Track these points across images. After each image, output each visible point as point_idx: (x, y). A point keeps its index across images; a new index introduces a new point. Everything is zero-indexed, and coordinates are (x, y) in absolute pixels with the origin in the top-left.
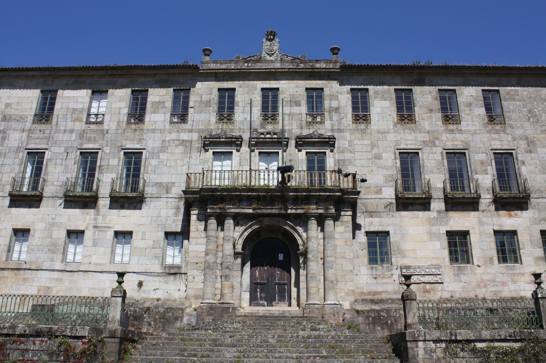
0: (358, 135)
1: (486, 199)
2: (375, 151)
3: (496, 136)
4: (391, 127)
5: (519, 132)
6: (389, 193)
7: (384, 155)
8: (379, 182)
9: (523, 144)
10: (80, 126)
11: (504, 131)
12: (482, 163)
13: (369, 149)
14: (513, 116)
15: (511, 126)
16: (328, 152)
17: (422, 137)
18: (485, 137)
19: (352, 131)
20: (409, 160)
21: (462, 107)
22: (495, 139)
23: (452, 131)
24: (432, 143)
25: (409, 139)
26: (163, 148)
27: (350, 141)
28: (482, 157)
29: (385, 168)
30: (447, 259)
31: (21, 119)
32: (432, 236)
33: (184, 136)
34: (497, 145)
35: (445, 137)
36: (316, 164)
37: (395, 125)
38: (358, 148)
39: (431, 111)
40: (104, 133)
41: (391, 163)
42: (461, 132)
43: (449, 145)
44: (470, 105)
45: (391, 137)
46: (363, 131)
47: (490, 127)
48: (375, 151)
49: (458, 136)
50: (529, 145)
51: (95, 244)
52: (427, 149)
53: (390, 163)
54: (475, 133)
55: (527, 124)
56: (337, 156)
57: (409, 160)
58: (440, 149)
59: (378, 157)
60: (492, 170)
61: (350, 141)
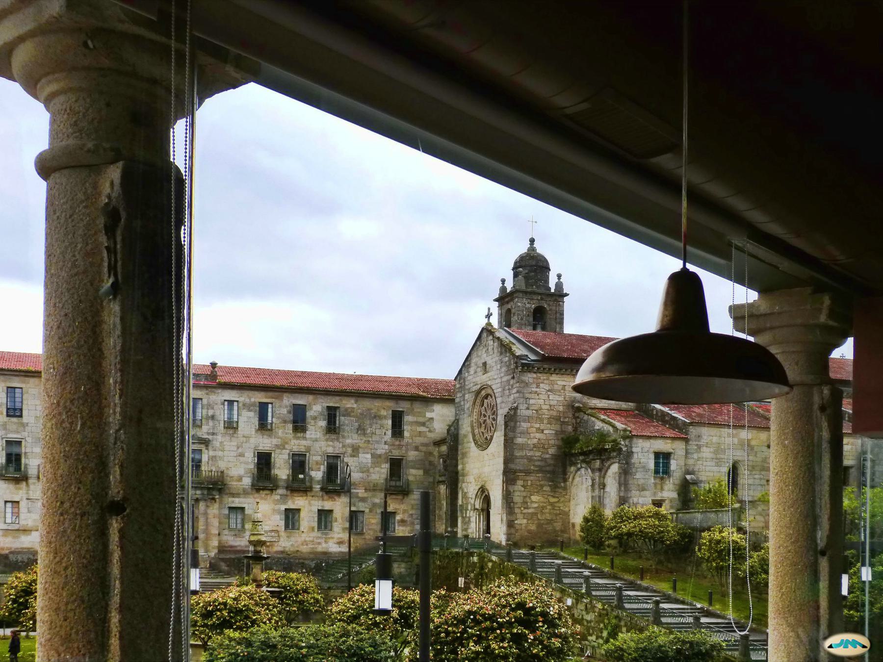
0: (228, 438)
2: (240, 450)
3: (331, 443)
4: (253, 433)
5: (348, 441)
7: (246, 454)
9: (349, 450)
11: (338, 439)
12: (317, 463)
13: (235, 449)
14: (346, 428)
15: (343, 437)
16: (204, 449)
17: (275, 441)
18: (323, 443)
19: (224, 435)
20: (264, 460)
21: (309, 420)
22: (329, 446)
23: (298, 438)
24: (281, 447)
25: (265, 443)
27: (221, 443)
28: (319, 458)
29: (247, 463)
30: (283, 528)
34: (330, 450)
35: (294, 442)
37: (257, 431)
38: (227, 448)
39: (285, 422)
41: (250, 461)
42: (305, 438)
43: (295, 449)
44: (315, 418)
45: (252, 440)
46: (232, 436)
47: (328, 436)
48: (240, 450)
49: (304, 442)
50: (353, 451)
51: (29, 512)
52: (278, 451)
53: (250, 460)
54: (316, 440)
55: (355, 436)
56: (211, 453)
57: (264, 460)
58: (288, 451)
59: (242, 455)
60: (323, 468)
61: (221, 443)
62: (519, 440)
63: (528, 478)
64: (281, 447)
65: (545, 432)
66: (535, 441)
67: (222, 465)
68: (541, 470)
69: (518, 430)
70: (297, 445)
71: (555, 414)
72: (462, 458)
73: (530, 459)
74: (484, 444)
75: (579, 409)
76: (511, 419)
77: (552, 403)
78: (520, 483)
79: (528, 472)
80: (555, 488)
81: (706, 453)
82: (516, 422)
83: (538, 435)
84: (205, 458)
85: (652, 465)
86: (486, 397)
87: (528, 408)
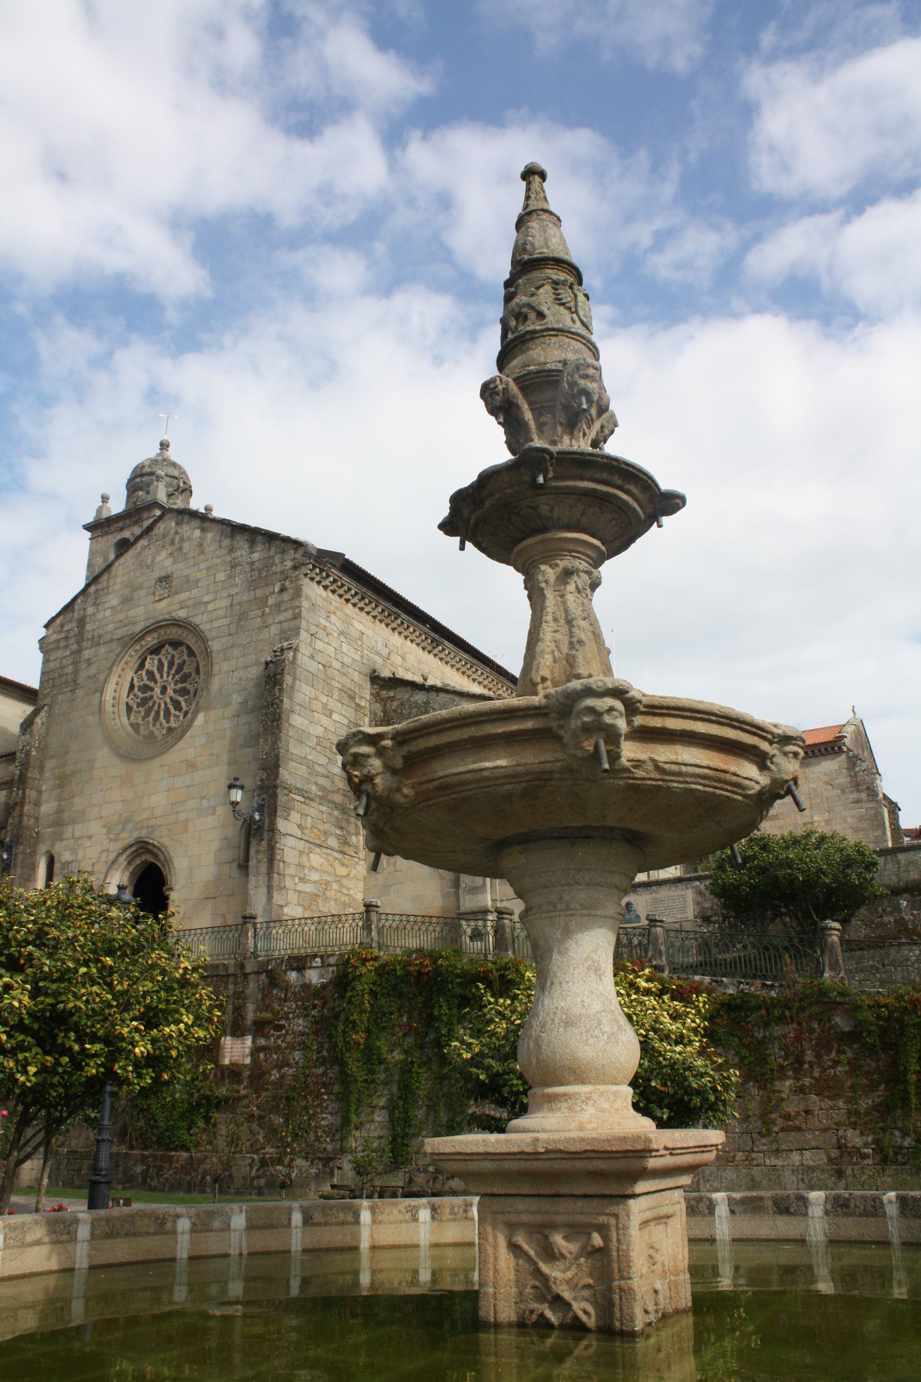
62: (297, 720)
63: (307, 810)
65: (335, 717)
66: (319, 731)
68: (324, 799)
69: (299, 697)
71: (348, 684)
72: (62, 781)
73: (310, 765)
76: (273, 678)
77: (347, 661)
78: (295, 817)
79: (308, 797)
82: (295, 678)
83: (325, 720)
86: (156, 650)
87: (312, 657)
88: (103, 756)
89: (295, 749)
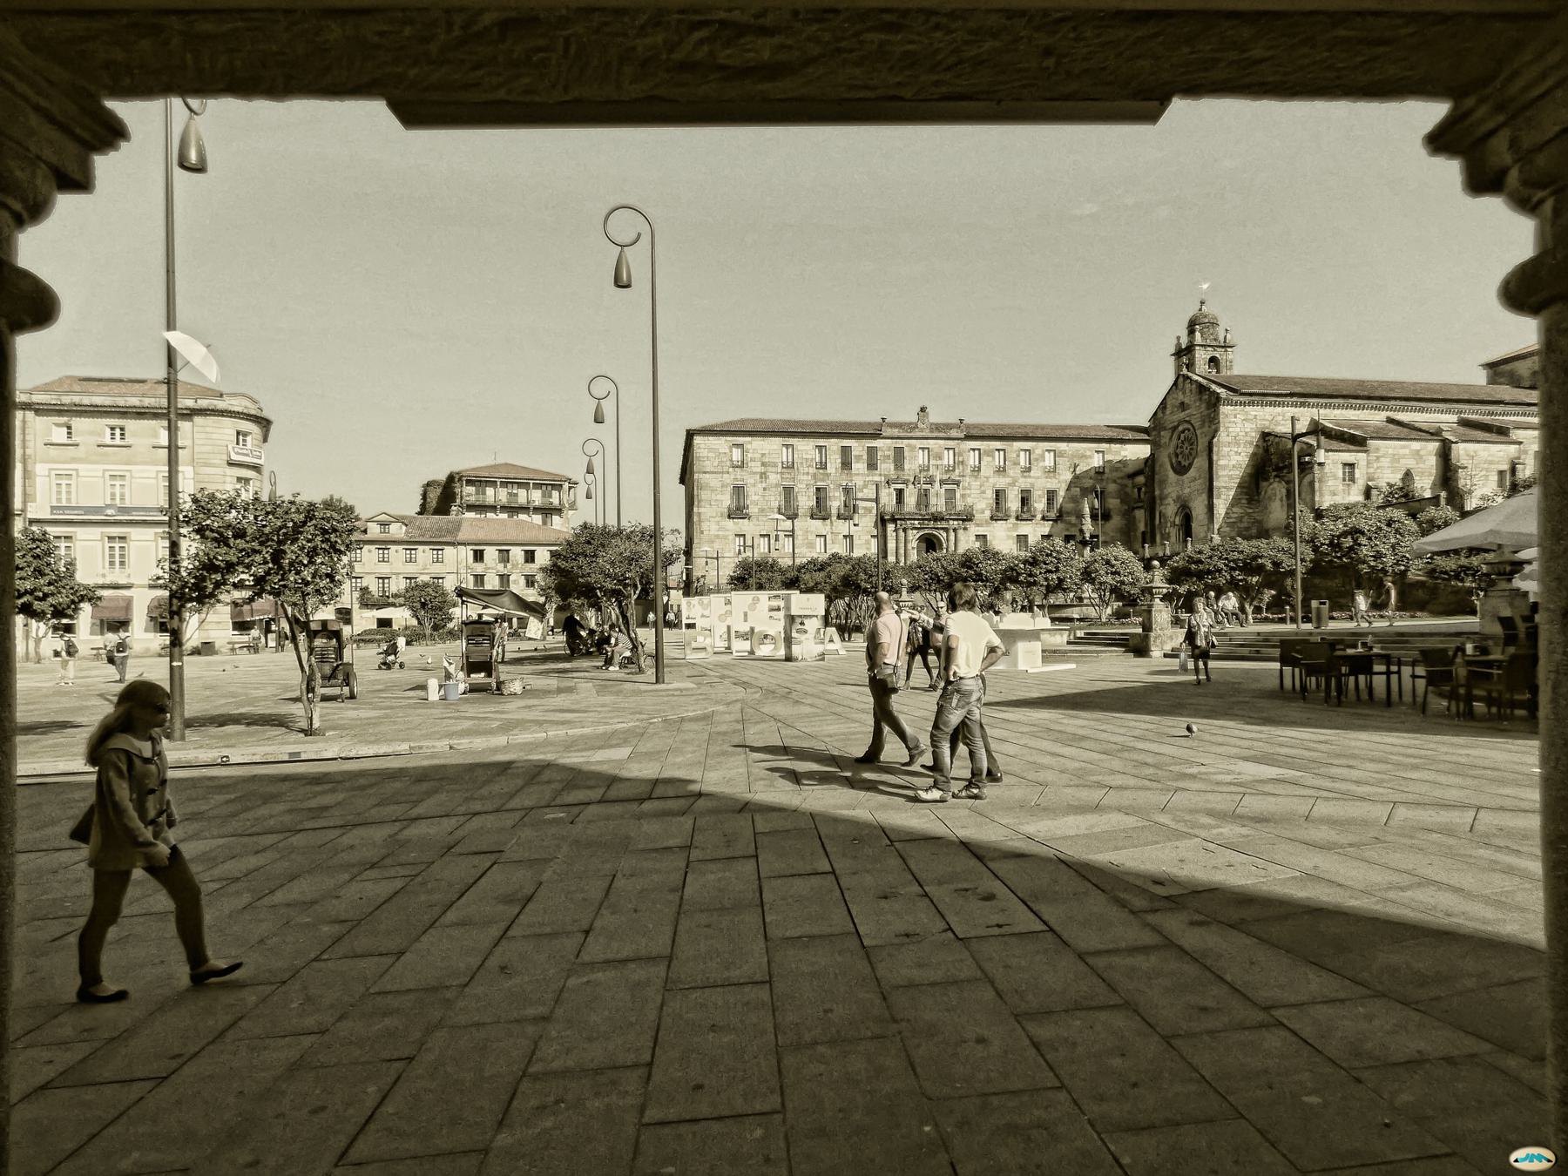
1: (1039, 516)
6: (988, 514)
8: (982, 505)
10: (812, 470)
17: (1009, 480)
24: (1013, 484)
25: (1001, 482)
26: (865, 486)
31: (775, 465)
32: (1009, 537)
33: (877, 478)
36: (951, 495)
40: (828, 475)
41: (990, 494)
57: (999, 495)
60: (1045, 500)
62: (1221, 462)
64: (1013, 484)
67: (969, 501)
70: (1024, 483)
74: (1181, 470)
75: (1269, 434)
80: (1250, 501)
81: (1385, 462)
84: (958, 495)
85: (1340, 474)
88: (1171, 474)
89: (1221, 473)
